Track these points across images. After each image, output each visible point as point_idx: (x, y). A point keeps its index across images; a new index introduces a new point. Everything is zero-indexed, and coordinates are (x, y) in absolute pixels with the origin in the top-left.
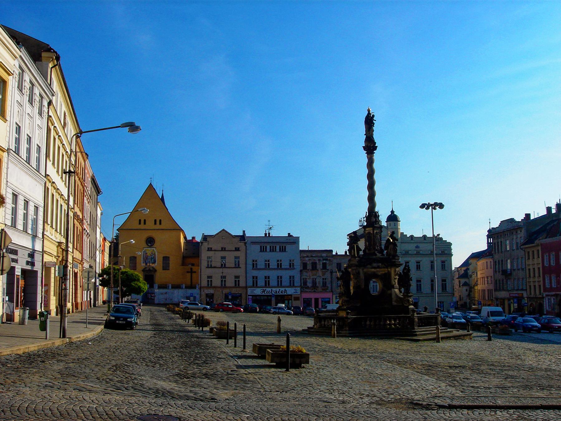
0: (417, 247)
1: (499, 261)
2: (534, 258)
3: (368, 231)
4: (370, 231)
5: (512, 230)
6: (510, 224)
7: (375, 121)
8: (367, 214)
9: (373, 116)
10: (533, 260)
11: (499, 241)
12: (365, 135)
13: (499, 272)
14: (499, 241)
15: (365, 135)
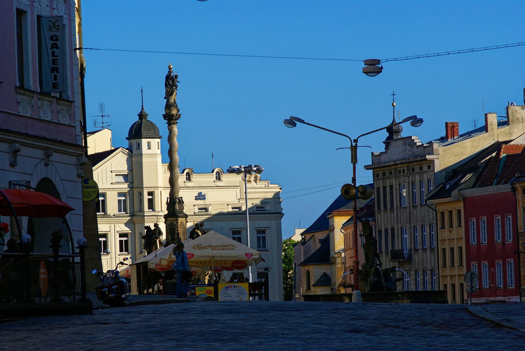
0: (200, 197)
1: (386, 231)
2: (451, 226)
3: (170, 222)
4: (172, 222)
5: (413, 162)
6: (408, 148)
7: (179, 82)
8: (169, 200)
9: (176, 77)
10: (451, 231)
11: (388, 184)
12: (165, 98)
13: (387, 254)
14: (388, 184)
15: (165, 98)
